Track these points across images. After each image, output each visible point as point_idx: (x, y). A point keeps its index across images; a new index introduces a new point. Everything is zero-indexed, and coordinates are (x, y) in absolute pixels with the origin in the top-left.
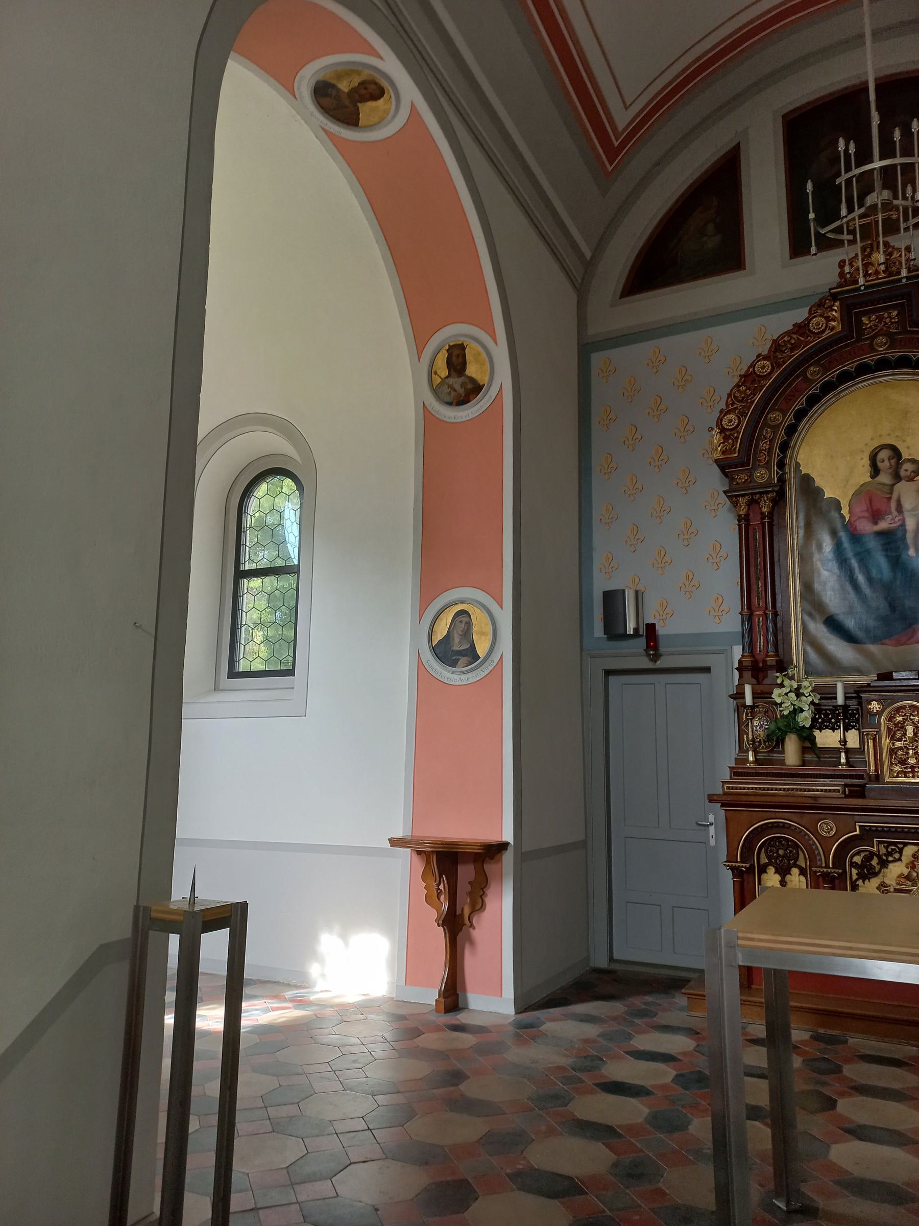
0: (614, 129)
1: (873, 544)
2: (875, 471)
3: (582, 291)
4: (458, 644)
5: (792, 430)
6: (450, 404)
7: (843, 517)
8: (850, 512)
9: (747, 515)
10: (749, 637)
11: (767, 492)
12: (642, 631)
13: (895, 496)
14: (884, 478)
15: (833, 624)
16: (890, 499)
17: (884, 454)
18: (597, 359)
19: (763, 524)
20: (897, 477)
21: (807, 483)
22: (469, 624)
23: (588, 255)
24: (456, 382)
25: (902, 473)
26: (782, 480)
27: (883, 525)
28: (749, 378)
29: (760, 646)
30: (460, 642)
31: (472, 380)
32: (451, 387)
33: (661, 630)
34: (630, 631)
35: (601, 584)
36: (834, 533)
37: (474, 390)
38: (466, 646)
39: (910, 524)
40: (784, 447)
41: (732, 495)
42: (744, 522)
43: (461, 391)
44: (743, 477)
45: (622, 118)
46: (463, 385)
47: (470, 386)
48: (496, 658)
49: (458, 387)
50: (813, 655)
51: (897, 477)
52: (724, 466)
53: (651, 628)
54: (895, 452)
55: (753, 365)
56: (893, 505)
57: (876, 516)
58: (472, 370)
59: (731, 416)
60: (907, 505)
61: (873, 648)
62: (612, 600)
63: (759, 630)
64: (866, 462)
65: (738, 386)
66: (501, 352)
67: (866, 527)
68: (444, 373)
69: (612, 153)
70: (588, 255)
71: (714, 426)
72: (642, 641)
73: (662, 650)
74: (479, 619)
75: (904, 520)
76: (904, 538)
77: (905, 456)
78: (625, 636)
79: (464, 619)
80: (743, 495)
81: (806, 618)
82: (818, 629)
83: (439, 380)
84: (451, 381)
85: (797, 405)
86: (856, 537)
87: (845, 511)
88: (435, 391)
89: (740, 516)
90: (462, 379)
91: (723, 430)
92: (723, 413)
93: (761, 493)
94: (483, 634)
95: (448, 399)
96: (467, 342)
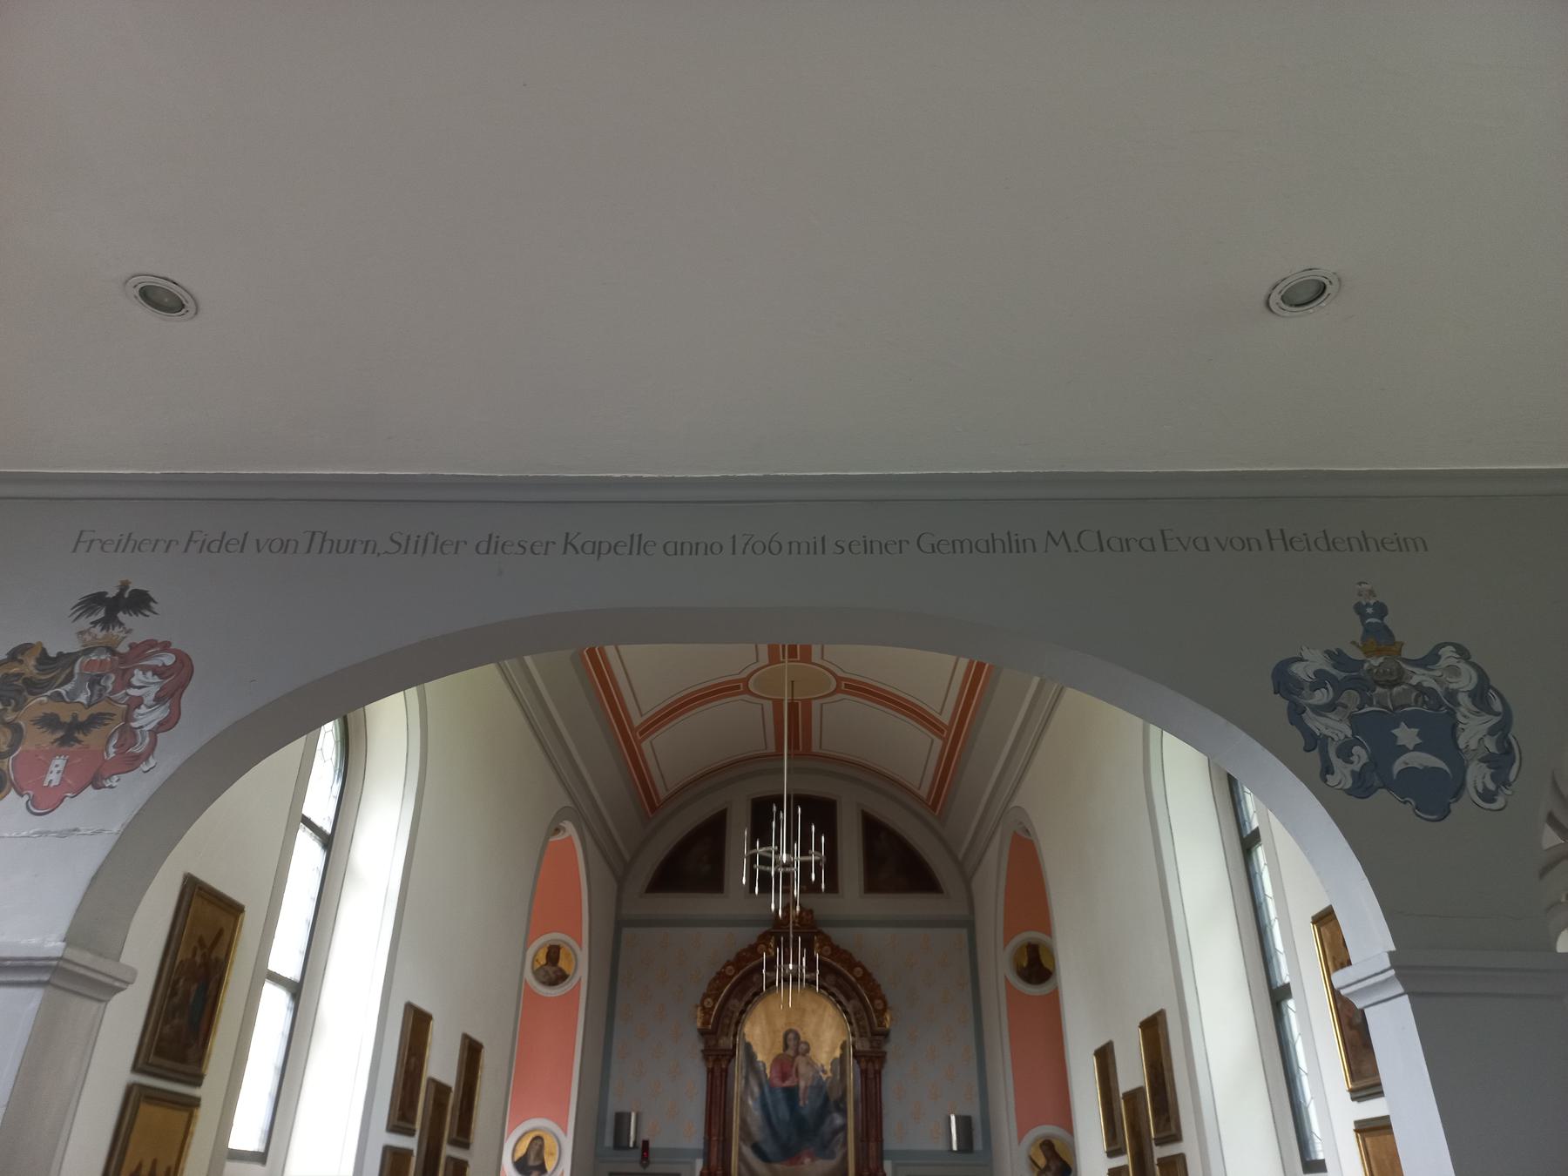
0: (658, 798)
1: (780, 1095)
2: (786, 1047)
3: (621, 883)
4: (532, 1162)
5: (743, 1012)
6: (543, 983)
7: (766, 1076)
8: (771, 1072)
9: (713, 1068)
10: (707, 1156)
11: (725, 1055)
12: (640, 1144)
13: (795, 1064)
14: (791, 1052)
15: (757, 1149)
16: (792, 1066)
17: (791, 1036)
18: (627, 932)
19: (721, 1076)
20: (797, 1053)
21: (748, 1047)
22: (542, 1147)
23: (627, 857)
24: (551, 969)
25: (800, 1050)
26: (734, 1046)
27: (787, 1083)
28: (721, 977)
29: (714, 1162)
30: (535, 1160)
31: (561, 970)
32: (547, 972)
33: (651, 1145)
34: (631, 1145)
35: (614, 1106)
36: (761, 1086)
37: (559, 978)
38: (537, 1163)
39: (802, 1084)
40: (737, 1023)
41: (706, 1054)
42: (711, 1072)
43: (553, 976)
44: (713, 1042)
45: (663, 794)
46: (555, 972)
47: (559, 974)
48: (559, 1172)
49: (551, 973)
50: (743, 1169)
51: (797, 1053)
52: (703, 1033)
53: (646, 1143)
54: (797, 1036)
55: (724, 967)
56: (794, 1070)
57: (784, 1077)
58: (562, 964)
59: (709, 1000)
60: (803, 1069)
61: (778, 1166)
62: (621, 1120)
63: (714, 1150)
64: (781, 1039)
65: (715, 979)
66: (583, 956)
67: (777, 1082)
68: (543, 961)
69: (653, 808)
70: (627, 857)
71: (699, 1003)
72: (639, 1152)
73: (651, 1159)
74: (549, 1143)
75: (798, 1082)
76: (798, 1094)
77: (802, 1039)
78: (628, 1148)
79: (539, 1142)
80: (711, 1055)
81: (742, 1143)
82: (747, 1151)
83: (538, 966)
84: (547, 968)
85: (746, 999)
86: (772, 1088)
87: (768, 1071)
88: (536, 973)
89: (708, 1068)
90: (554, 968)
91: (704, 1008)
92: (705, 996)
93: (723, 1055)
94: (552, 1154)
95: (544, 980)
96: (562, 944)
